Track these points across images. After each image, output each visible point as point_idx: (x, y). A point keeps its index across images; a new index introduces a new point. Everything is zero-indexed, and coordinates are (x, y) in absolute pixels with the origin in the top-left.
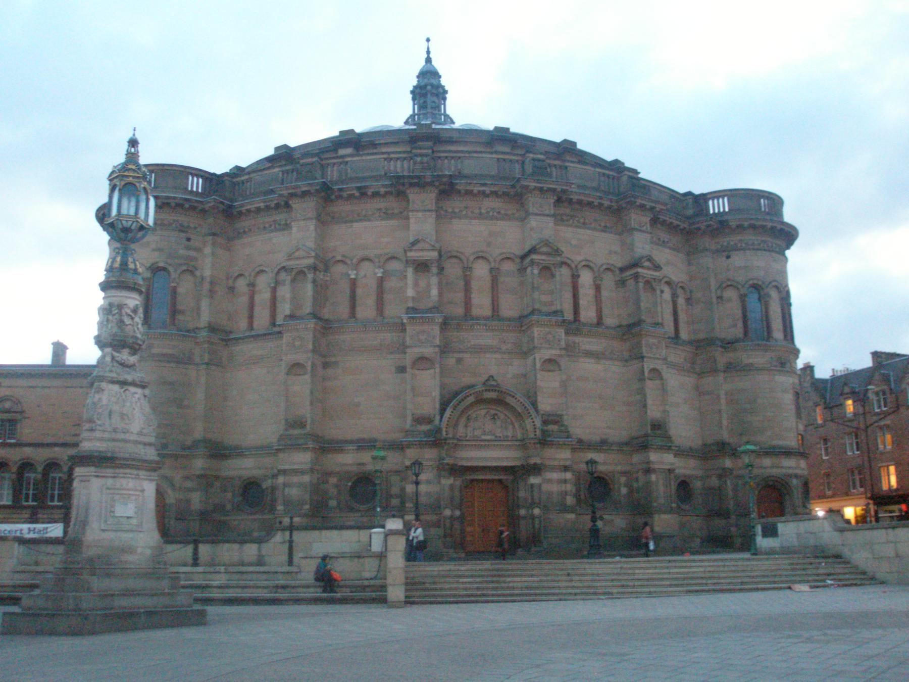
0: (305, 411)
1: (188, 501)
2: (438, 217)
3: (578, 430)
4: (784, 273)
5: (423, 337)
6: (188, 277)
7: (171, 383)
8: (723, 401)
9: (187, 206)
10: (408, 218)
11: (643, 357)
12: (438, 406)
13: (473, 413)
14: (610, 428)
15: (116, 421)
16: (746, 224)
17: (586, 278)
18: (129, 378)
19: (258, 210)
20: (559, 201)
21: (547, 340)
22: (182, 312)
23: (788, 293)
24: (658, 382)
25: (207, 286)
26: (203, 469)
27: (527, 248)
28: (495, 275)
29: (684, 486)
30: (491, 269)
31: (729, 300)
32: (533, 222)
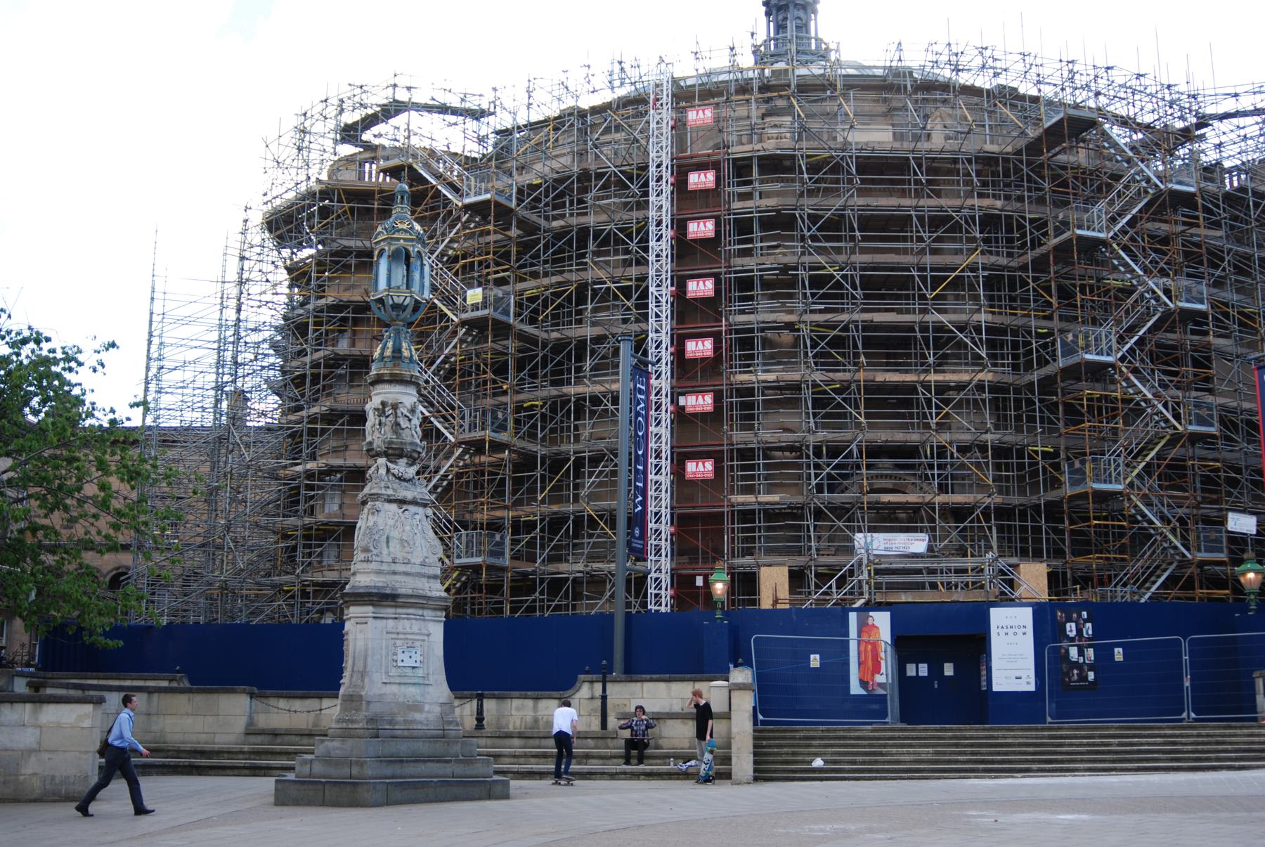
15: (395, 548)
18: (409, 495)
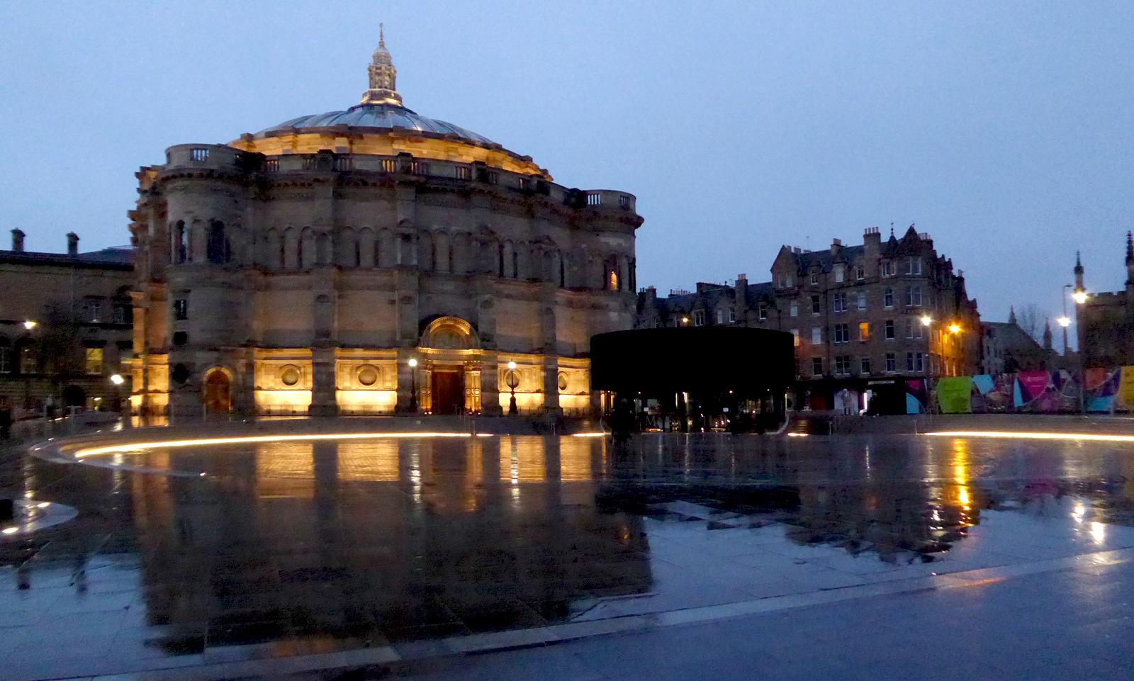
4: (632, 247)
17: (508, 249)
23: (634, 260)
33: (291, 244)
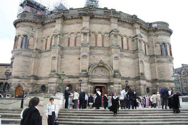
0: (56, 68)
1: (29, 90)
2: (90, 23)
3: (123, 75)
4: (170, 41)
5: (85, 50)
6: (32, 38)
7: (26, 62)
8: (157, 69)
9: (32, 21)
10: (82, 24)
11: (138, 58)
12: (88, 67)
13: (97, 69)
14: (131, 74)
16: (161, 29)
17: (125, 39)
19: (49, 23)
20: (118, 21)
21: (115, 52)
22: (30, 45)
24: (142, 64)
25: (36, 40)
26: (32, 82)
27: (111, 30)
28: (103, 37)
29: (148, 89)
30: (102, 36)
31: (158, 46)
32: (112, 25)
33: (49, 42)
